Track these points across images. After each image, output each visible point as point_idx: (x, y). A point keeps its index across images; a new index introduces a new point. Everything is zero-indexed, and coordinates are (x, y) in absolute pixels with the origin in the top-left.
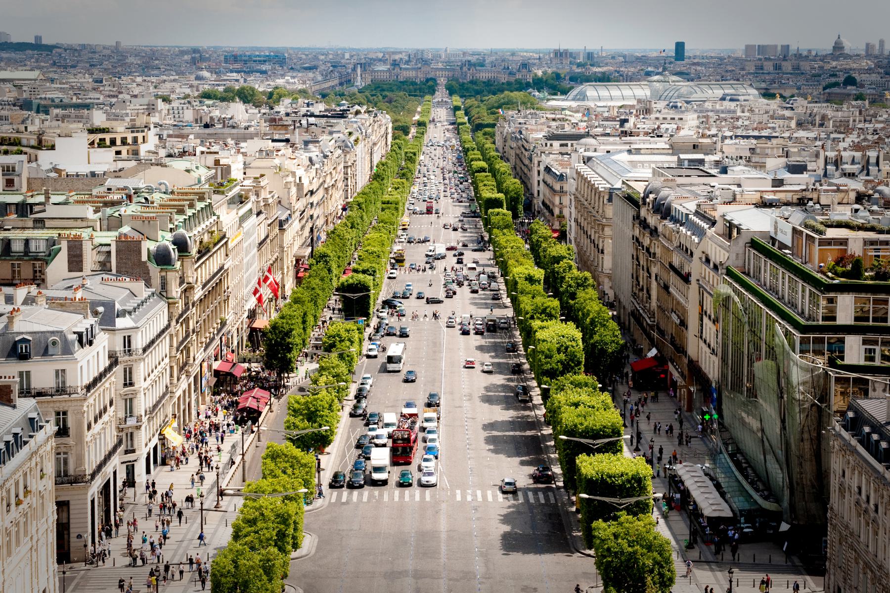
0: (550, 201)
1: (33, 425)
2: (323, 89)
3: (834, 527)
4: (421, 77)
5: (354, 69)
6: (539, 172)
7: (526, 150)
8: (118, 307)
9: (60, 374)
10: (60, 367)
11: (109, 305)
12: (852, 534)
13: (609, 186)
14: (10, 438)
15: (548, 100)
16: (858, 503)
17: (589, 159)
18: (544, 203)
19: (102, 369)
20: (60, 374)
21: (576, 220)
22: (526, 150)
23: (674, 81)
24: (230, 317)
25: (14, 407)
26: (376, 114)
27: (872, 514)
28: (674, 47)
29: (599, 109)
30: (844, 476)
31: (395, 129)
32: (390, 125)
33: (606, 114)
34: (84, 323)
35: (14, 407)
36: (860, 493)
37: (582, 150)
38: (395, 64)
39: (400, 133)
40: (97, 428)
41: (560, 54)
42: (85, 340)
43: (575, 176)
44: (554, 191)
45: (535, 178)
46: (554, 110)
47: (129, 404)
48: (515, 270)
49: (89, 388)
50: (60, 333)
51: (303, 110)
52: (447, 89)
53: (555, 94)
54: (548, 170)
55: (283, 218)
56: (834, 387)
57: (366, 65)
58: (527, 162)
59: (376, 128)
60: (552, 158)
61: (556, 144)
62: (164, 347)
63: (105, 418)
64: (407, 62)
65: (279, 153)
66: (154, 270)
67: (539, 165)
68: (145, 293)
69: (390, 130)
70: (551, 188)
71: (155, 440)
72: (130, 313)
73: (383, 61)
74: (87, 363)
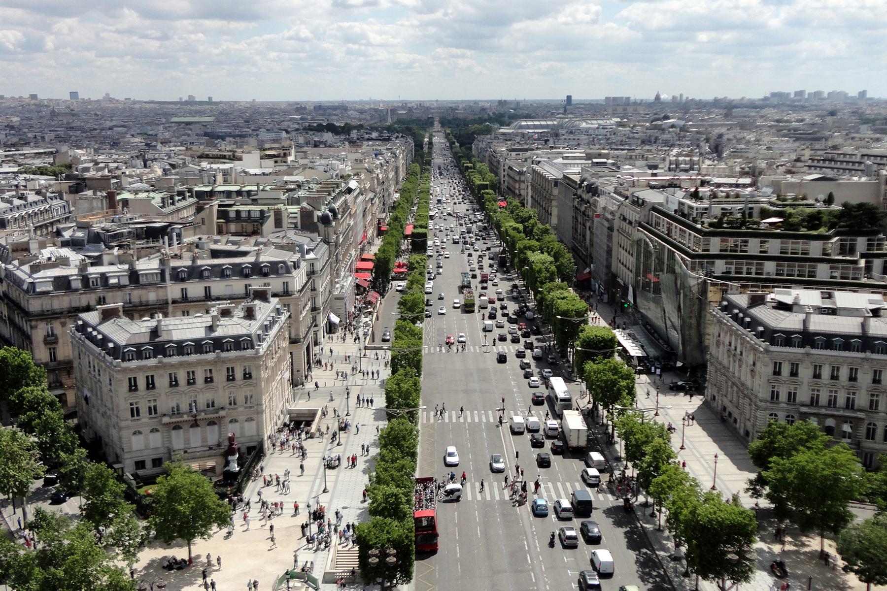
1: (278, 312)
3: (712, 364)
8: (306, 247)
9: (286, 284)
10: (285, 280)
11: (301, 246)
12: (724, 367)
14: (271, 319)
16: (729, 351)
19: (304, 282)
20: (286, 284)
24: (353, 252)
25: (269, 302)
27: (739, 357)
30: (719, 336)
34: (296, 257)
35: (269, 302)
36: (730, 345)
40: (304, 313)
42: (296, 266)
47: (314, 299)
49: (300, 291)
50: (284, 262)
56: (710, 288)
62: (328, 270)
63: (307, 308)
66: (321, 226)
68: (319, 239)
71: (326, 320)
72: (312, 250)
74: (298, 278)
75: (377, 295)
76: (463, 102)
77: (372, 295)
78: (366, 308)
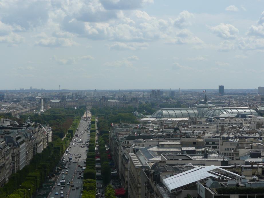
5: (40, 102)
13: (141, 165)
15: (142, 117)
17: (137, 150)
23: (210, 107)
26: (40, 127)
28: (218, 88)
31: (53, 134)
32: (51, 132)
33: (170, 126)
38: (63, 99)
41: (156, 93)
53: (147, 114)
59: (39, 134)
61: (131, 142)
69: (50, 136)
73: (57, 97)
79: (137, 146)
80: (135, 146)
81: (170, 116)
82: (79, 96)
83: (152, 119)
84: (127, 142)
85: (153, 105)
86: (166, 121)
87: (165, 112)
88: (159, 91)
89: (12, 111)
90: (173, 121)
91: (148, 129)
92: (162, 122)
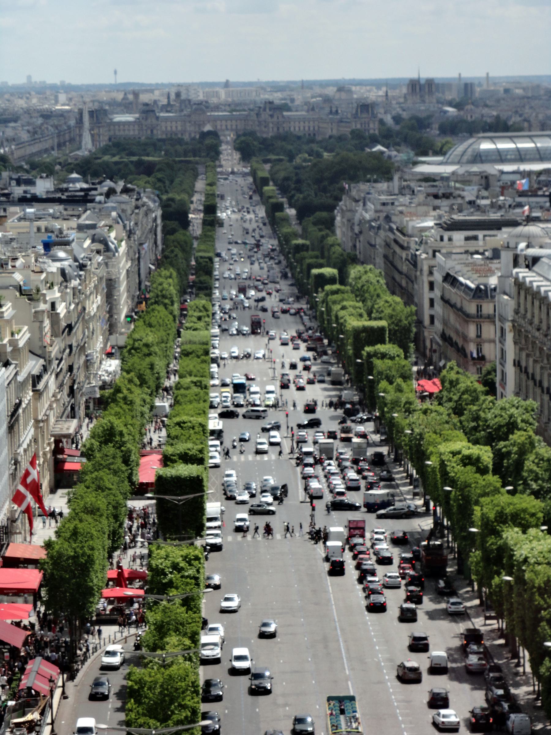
0: (457, 332)
2: (33, 155)
4: (190, 132)
5: (80, 121)
6: (432, 286)
7: (402, 247)
15: (415, 163)
17: (536, 260)
18: (444, 336)
21: (517, 364)
22: (402, 247)
26: (139, 193)
29: (505, 178)
31: (164, 217)
32: (159, 213)
37: (522, 245)
38: (148, 110)
39: (173, 224)
41: (419, 88)
43: (513, 290)
44: (466, 317)
45: (427, 295)
46: (428, 179)
48: (445, 448)
51: (18, 191)
52: (237, 149)
53: (425, 154)
54: (450, 279)
55: (36, 372)
57: (98, 115)
58: (404, 268)
60: (460, 260)
61: (459, 236)
64: (167, 108)
65: (18, 263)
67: (431, 273)
69: (159, 221)
70: (460, 311)
73: (126, 106)
75: (52, 671)
76: (305, 85)
77: (38, 673)
78: (21, 710)
79: (533, 247)
80: (528, 247)
81: (501, 157)
82: (181, 101)
83: (448, 169)
84: (446, 238)
85: (421, 123)
86: (502, 172)
87: (486, 146)
88: (430, 83)
89: (7, 149)
90: (524, 171)
91: (463, 198)
92: (486, 177)
